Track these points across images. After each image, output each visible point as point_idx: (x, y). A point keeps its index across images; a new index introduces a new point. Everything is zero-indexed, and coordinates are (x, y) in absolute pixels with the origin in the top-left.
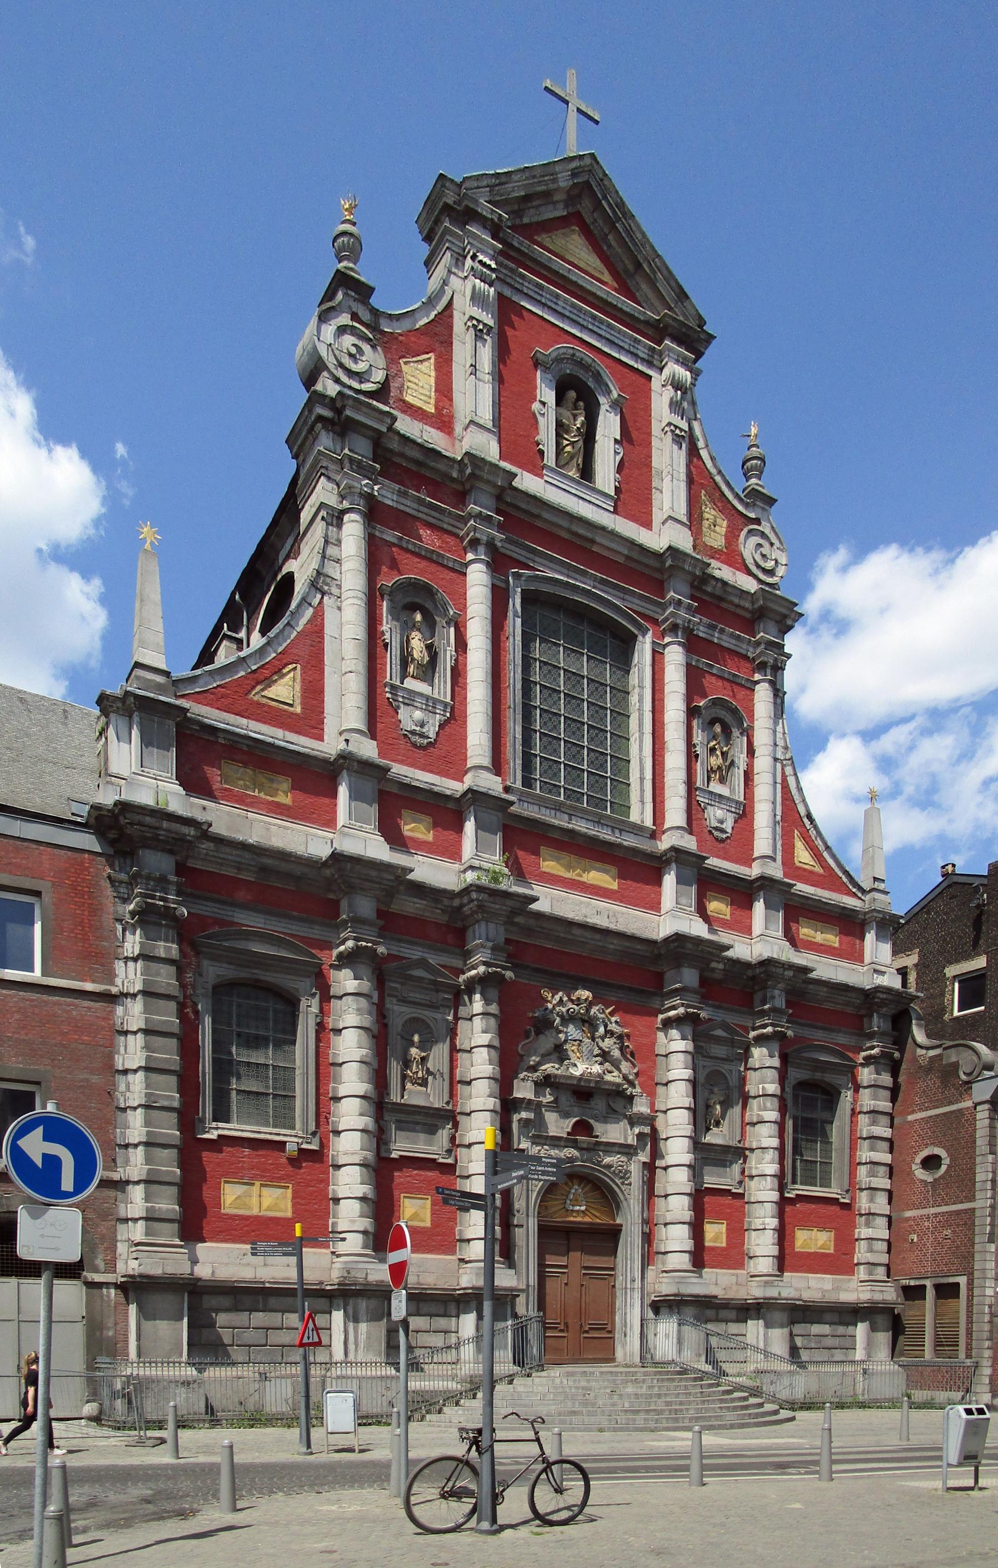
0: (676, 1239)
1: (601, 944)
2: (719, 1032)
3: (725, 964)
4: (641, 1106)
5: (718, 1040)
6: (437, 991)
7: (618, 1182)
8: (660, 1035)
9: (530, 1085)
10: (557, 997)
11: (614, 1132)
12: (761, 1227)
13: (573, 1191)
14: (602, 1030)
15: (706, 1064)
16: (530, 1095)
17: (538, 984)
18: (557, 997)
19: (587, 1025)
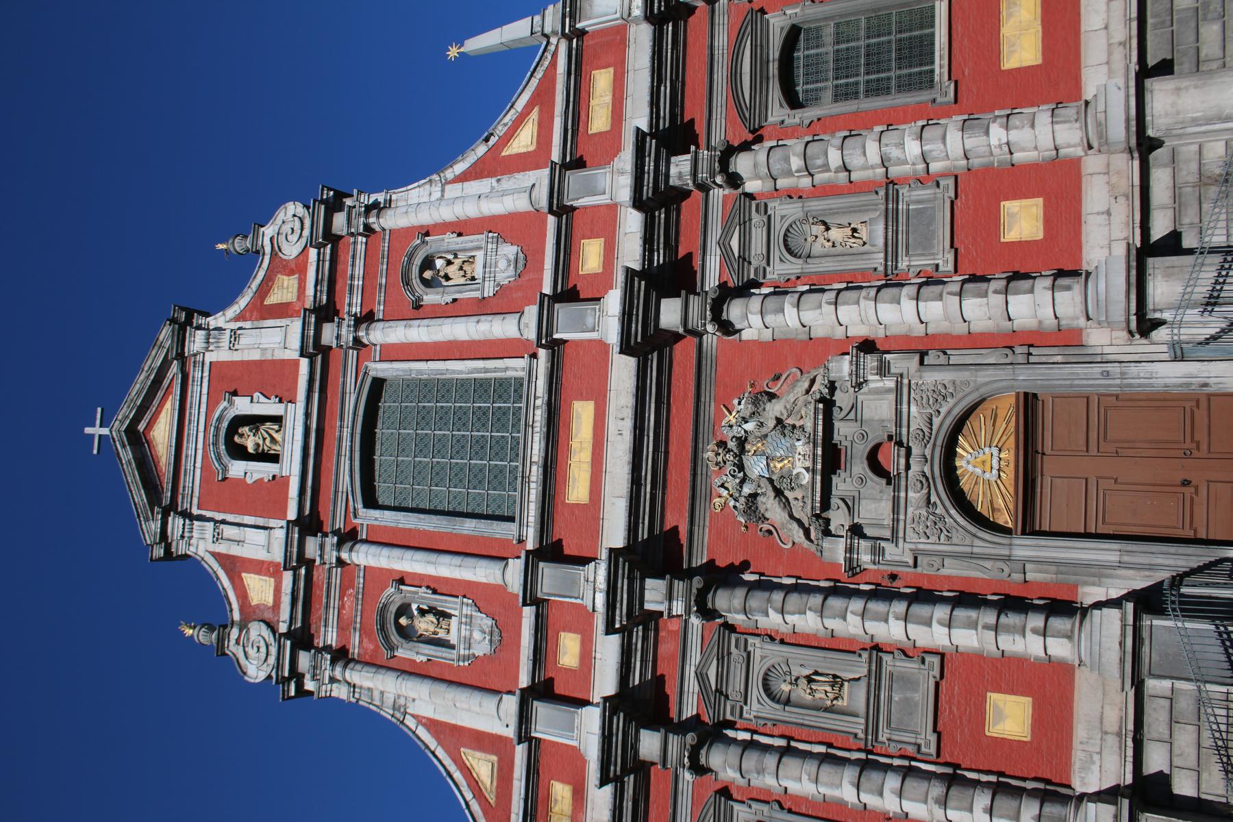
0: (1031, 307)
2: (735, 243)
4: (841, 371)
5: (745, 244)
7: (951, 401)
8: (747, 335)
9: (827, 543)
11: (877, 406)
12: (1006, 149)
13: (970, 468)
15: (777, 259)
16: (841, 545)
17: (708, 514)
19: (748, 447)
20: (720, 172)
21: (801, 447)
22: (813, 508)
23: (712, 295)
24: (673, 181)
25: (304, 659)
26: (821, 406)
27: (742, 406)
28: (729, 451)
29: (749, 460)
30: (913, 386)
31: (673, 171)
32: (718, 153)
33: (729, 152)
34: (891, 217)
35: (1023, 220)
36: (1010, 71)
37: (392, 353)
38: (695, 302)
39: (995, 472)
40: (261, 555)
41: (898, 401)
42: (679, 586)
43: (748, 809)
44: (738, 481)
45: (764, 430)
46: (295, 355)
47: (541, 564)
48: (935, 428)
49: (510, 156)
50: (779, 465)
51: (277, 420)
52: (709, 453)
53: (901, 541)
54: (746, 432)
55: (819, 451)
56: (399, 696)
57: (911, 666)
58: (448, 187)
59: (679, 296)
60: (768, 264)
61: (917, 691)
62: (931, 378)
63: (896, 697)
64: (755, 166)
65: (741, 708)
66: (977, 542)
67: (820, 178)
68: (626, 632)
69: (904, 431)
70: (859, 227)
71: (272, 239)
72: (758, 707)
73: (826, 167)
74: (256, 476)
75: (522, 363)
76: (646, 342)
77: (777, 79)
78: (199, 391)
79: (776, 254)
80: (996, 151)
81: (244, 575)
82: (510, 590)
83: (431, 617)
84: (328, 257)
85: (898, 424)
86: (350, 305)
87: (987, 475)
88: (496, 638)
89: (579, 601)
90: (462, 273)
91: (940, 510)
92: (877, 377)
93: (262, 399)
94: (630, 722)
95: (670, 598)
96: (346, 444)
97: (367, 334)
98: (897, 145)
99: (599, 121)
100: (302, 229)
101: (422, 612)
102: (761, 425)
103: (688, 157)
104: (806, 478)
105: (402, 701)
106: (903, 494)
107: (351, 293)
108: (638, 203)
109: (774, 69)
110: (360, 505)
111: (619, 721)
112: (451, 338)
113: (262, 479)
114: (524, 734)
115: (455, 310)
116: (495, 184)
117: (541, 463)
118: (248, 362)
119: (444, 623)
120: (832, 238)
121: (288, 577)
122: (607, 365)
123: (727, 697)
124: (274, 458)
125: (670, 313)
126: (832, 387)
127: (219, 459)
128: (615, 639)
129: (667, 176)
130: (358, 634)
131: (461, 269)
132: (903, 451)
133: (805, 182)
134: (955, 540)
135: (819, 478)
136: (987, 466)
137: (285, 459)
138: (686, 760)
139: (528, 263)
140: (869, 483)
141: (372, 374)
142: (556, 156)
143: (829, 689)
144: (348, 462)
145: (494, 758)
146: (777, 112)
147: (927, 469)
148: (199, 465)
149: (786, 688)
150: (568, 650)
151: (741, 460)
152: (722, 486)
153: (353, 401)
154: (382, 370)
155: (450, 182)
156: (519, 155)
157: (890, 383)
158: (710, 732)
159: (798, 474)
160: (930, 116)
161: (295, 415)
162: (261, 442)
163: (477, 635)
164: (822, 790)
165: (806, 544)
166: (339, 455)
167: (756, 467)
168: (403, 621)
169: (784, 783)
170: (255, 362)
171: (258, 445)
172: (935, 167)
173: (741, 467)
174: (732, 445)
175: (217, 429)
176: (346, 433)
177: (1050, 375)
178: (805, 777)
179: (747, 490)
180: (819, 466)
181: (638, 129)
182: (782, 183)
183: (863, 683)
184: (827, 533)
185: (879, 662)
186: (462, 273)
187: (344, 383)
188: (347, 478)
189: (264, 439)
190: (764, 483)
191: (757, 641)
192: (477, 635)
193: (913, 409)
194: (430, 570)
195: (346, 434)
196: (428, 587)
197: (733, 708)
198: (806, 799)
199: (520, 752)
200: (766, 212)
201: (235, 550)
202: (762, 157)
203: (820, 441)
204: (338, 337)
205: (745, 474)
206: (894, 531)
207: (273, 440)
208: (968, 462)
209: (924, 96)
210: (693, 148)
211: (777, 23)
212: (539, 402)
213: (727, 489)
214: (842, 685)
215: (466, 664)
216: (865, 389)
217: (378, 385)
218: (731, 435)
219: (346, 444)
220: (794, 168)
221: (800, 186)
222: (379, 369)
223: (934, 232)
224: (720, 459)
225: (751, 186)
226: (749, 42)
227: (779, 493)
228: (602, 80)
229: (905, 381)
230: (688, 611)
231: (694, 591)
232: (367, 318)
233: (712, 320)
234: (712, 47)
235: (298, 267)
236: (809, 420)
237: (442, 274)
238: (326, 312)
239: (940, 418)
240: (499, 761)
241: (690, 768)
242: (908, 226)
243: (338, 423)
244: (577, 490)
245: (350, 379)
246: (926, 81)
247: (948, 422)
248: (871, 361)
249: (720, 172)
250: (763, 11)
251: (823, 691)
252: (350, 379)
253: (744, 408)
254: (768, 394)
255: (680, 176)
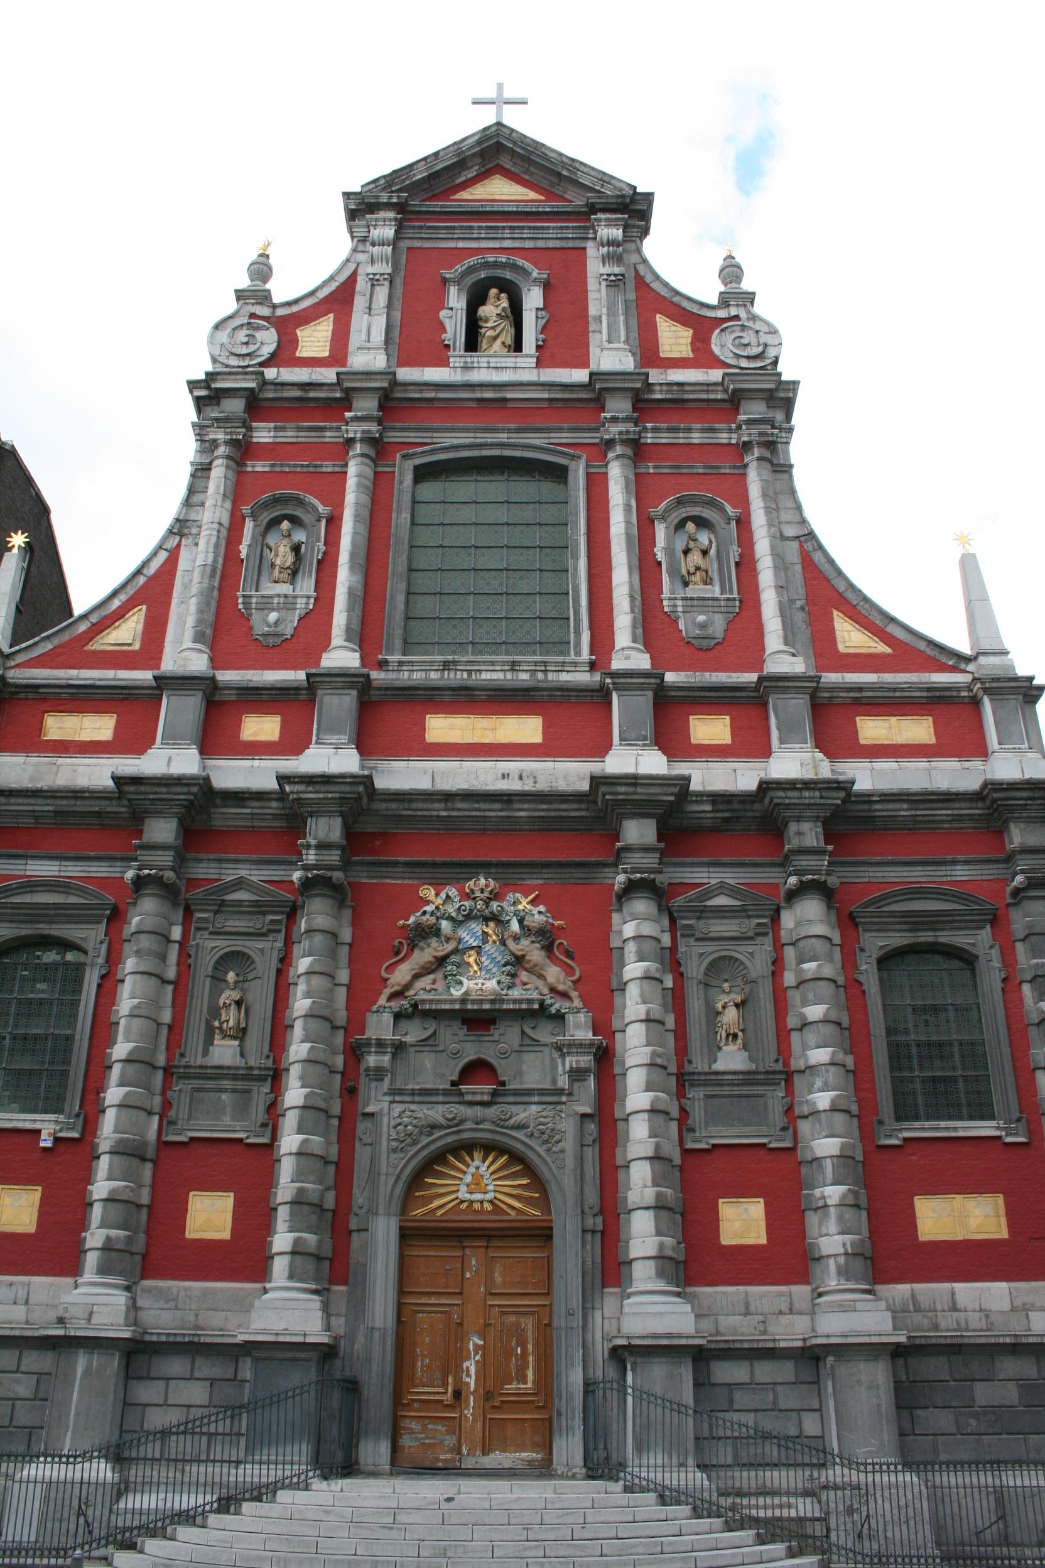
0: (643, 1236)
1: (503, 814)
2: (722, 901)
3: (713, 803)
4: (577, 1026)
5: (721, 913)
6: (264, 913)
9: (387, 1018)
10: (443, 895)
12: (821, 1203)
13: (472, 1170)
14: (515, 926)
16: (388, 1035)
17: (416, 882)
18: (443, 895)
19: (492, 924)
20: (801, 882)
21: (491, 985)
22: (423, 1001)
23: (660, 879)
24: (793, 827)
25: (235, 406)
26: (536, 1006)
27: (537, 916)
28: (487, 904)
29: (477, 927)
30: (559, 1107)
31: (806, 826)
32: (823, 878)
33: (827, 893)
34: (748, 1078)
35: (743, 1221)
36: (912, 1206)
37: (597, 486)
38: (650, 860)
39: (468, 1196)
40: (356, 337)
41: (542, 1092)
42: (334, 857)
43: (99, 941)
44: (454, 914)
45: (510, 943)
46: (593, 367)
47: (354, 693)
48: (513, 1133)
49: (832, 620)
50: (471, 960)
51: (517, 346)
52: (482, 883)
53: (390, 1098)
54: (508, 921)
55: (486, 1006)
56: (200, 527)
57: (258, 1112)
58: (795, 545)
59: (659, 841)
60: (697, 940)
61: (233, 1119)
62: (568, 1127)
63: (224, 1097)
64: (809, 922)
65: (207, 929)
66: (392, 1180)
67: (794, 997)
68: (282, 795)
69: (511, 1099)
70: (739, 1041)
71: (737, 318)
72: (210, 948)
73: (805, 1003)
74: (449, 325)
75: (585, 655)
76: (608, 802)
77: (913, 940)
78: (552, 235)
79: (709, 948)
80: (817, 1192)
81: (331, 315)
82: (325, 655)
83: (290, 559)
84: (712, 396)
85: (516, 1093)
86: (655, 430)
87: (463, 1188)
88: (271, 641)
89: (314, 738)
90: (692, 570)
91: (425, 1140)
92: (567, 1067)
93: (542, 322)
94: (184, 806)
95: (322, 846)
96: (490, 438)
97: (618, 457)
98: (826, 1083)
99: (872, 729)
100: (748, 357)
101: (296, 549)
102: (516, 938)
103: (822, 843)
104: (457, 993)
105: (194, 531)
106: (440, 1099)
107: (670, 430)
108: (765, 786)
109: (925, 937)
110: (418, 461)
111: (182, 794)
112: (614, 564)
113: (445, 331)
114: (164, 683)
115: (647, 569)
116: (799, 604)
117: (470, 683)
118: (586, 299)
119: (285, 576)
120: (727, 1011)
121: (328, 375)
122: (582, 756)
123: (216, 912)
124: (472, 344)
125: (638, 832)
126: (560, 1017)
127: (471, 270)
128: (272, 784)
129: (798, 819)
130: (267, 469)
131: (698, 568)
132: (486, 1098)
133: (789, 979)
134: (393, 1156)
135: (457, 1007)
136: (476, 1187)
137: (473, 358)
138: (147, 872)
139: (703, 652)
140: (453, 1062)
141: (572, 465)
142: (831, 678)
143: (231, 1024)
144: (467, 441)
145: (137, 646)
146: (875, 943)
147: (469, 1125)
148: (461, 244)
149: (231, 976)
150: (261, 727)
151: (475, 918)
152: (448, 897)
153: (535, 443)
154: (576, 478)
155: (801, 546)
156: (832, 631)
157: (563, 1082)
158: (179, 895)
159: (461, 983)
160: (863, 1115)
161: (522, 369)
162: (490, 324)
163: (273, 616)
164: (123, 1022)
165: (387, 992)
166: (475, 430)
167: (470, 935)
168: (285, 525)
169: (129, 980)
170: (586, 308)
171: (486, 321)
172: (804, 1127)
173: (469, 917)
174: (494, 905)
175: (504, 266)
176: (503, 437)
177: (570, 1254)
178: (136, 1001)
179: (445, 925)
180: (469, 1007)
181: (853, 783)
182: (789, 953)
183: (238, 1062)
184: (398, 1016)
185: (261, 1079)
186: (692, 570)
187: (560, 430)
188: (449, 442)
189: (493, 328)
190: (450, 947)
191: (280, 944)
192: (273, 616)
193: (534, 1108)
194: (344, 557)
195: (502, 439)
196: (325, 553)
197: (206, 920)
198: (113, 1004)
199: (145, 676)
200: (757, 934)
201: (360, 303)
202: (819, 929)
203: (497, 1006)
204: (614, 420)
205: (462, 922)
206: (401, 1092)
207: (495, 338)
208: (480, 1167)
209: (886, 1108)
210: (830, 848)
211: (980, 940)
212: (540, 676)
213: (445, 902)
214: (235, 1038)
215: (241, 606)
216: (556, 1055)
217: (559, 474)
218: (504, 904)
219: (490, 438)
220: (805, 966)
221: (786, 974)
222: (579, 473)
223: (732, 1125)
224: (478, 894)
225: (787, 920)
226: (957, 907)
227: (441, 961)
228: (918, 730)
229: (564, 1099)
230: (306, 868)
231: (329, 874)
232: (638, 451)
233: (630, 880)
234: (954, 862)
235: (702, 356)
236: (521, 993)
237: (692, 545)
238: (644, 403)
239: (523, 1138)
240: (133, 652)
241: (138, 876)
242: (740, 1096)
243: (513, 426)
244: (441, 728)
245: (566, 437)
246: (904, 1112)
247: (519, 1146)
248: (586, 1060)
249: (801, 882)
250: (994, 922)
251: (231, 1018)
252: (566, 437)
253: (538, 916)
254: (552, 944)
255: (800, 833)
